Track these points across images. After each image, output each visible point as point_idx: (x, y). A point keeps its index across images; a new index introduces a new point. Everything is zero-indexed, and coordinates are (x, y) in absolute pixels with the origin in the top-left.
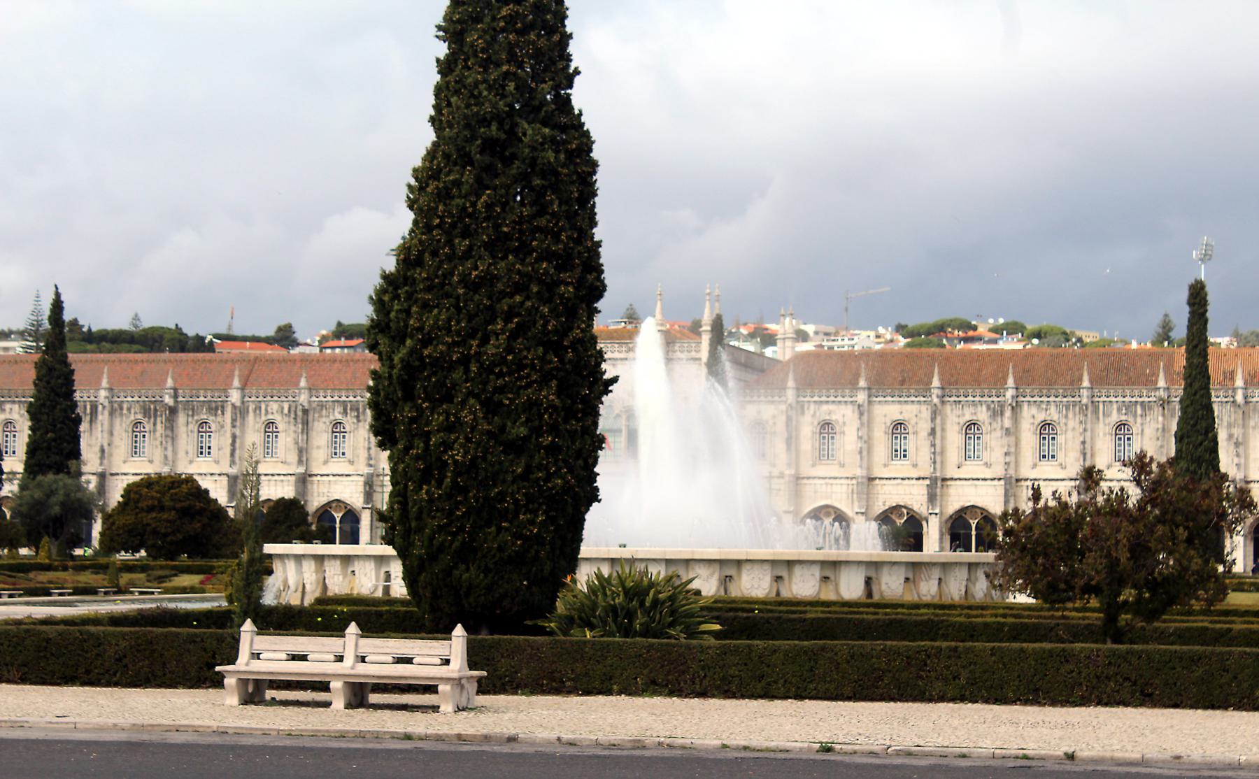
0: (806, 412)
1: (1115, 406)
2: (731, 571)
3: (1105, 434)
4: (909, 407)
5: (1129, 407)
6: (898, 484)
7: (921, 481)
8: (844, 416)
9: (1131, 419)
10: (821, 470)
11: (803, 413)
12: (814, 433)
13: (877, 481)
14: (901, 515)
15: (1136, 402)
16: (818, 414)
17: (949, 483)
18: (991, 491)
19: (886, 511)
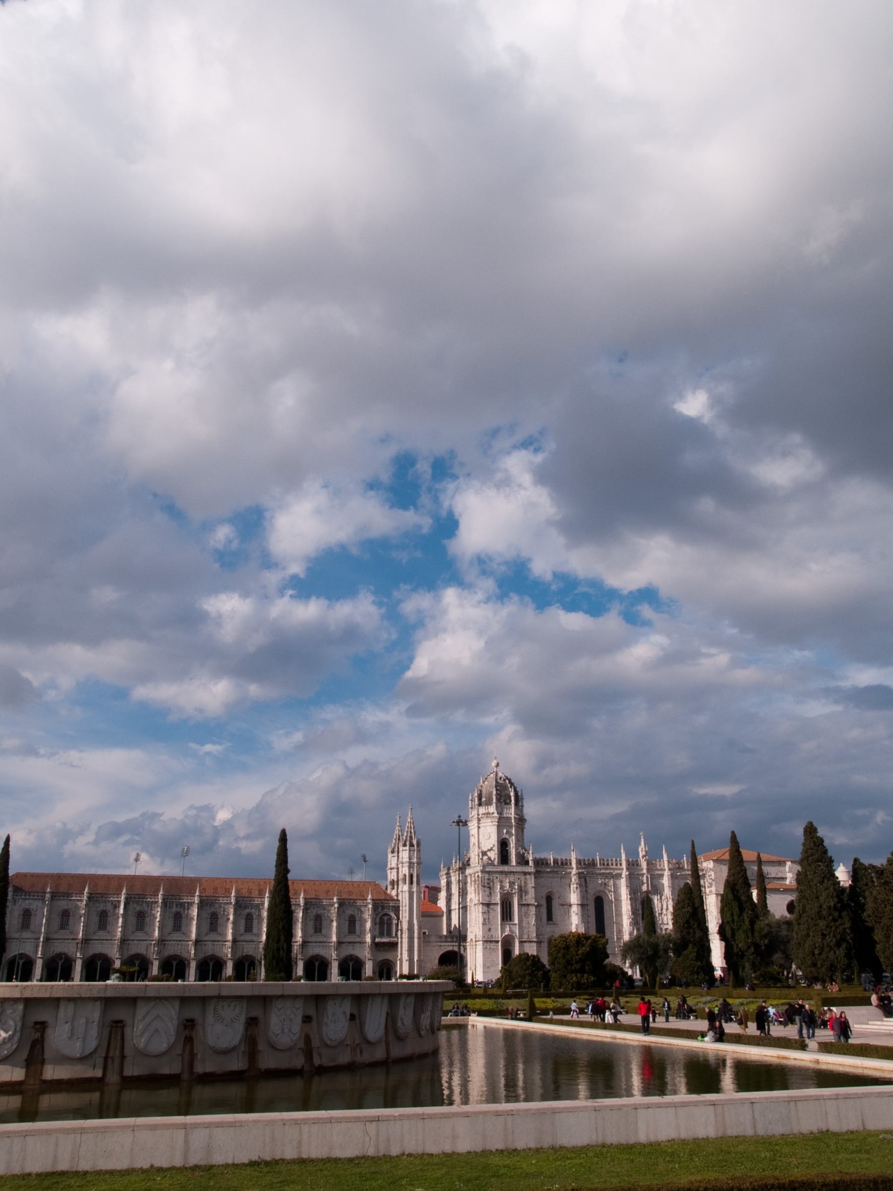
0: (17, 904)
1: (175, 904)
2: (193, 1012)
3: (169, 917)
6: (61, 942)
7: (74, 941)
8: (37, 906)
9: (182, 910)
11: (15, 905)
12: (20, 915)
13: (51, 941)
14: (61, 959)
15: (185, 902)
16: (23, 904)
17: (88, 942)
19: (53, 957)
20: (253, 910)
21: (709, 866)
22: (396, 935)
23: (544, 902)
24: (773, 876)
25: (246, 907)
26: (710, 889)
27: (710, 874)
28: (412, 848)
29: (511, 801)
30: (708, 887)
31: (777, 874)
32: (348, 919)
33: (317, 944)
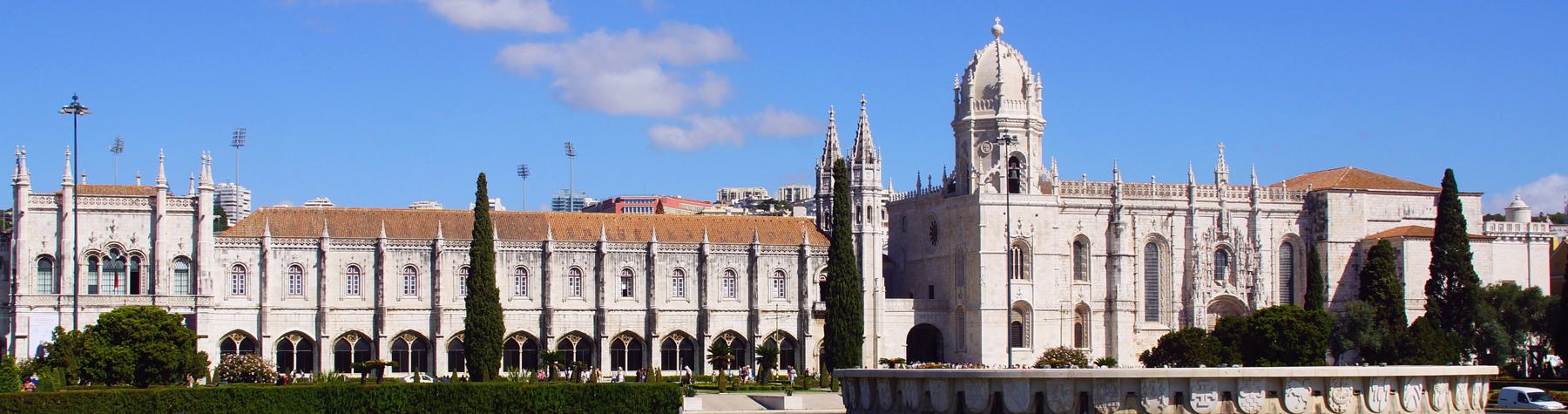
1: (514, 254)
4: (360, 253)
5: (525, 254)
10: (289, 303)
11: (275, 257)
14: (353, 339)
16: (287, 257)
18: (424, 317)
20: (631, 264)
21: (1320, 198)
23: (1070, 251)
24: (1417, 216)
25: (623, 256)
26: (1318, 235)
27: (1321, 210)
28: (870, 166)
30: (1317, 231)
31: (1423, 212)
32: (773, 275)
33: (729, 313)
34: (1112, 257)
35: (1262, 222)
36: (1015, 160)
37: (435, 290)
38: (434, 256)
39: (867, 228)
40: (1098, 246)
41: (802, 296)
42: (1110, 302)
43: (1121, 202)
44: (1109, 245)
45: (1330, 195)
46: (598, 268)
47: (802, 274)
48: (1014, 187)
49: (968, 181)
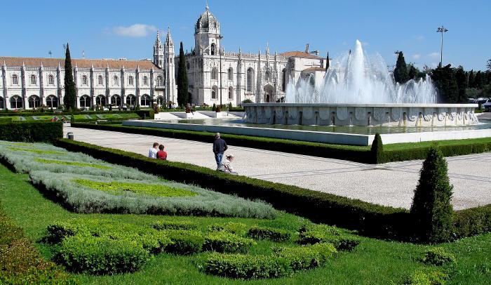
22: (164, 84)
23: (227, 71)
29: (215, 26)
34: (239, 74)
35: (277, 65)
36: (213, 45)
37: (41, 82)
38: (40, 73)
39: (170, 64)
40: (235, 71)
41: (152, 84)
42: (238, 86)
43: (241, 58)
44: (238, 70)
45: (296, 59)
46: (91, 76)
47: (151, 78)
48: (213, 53)
49: (199, 51)
